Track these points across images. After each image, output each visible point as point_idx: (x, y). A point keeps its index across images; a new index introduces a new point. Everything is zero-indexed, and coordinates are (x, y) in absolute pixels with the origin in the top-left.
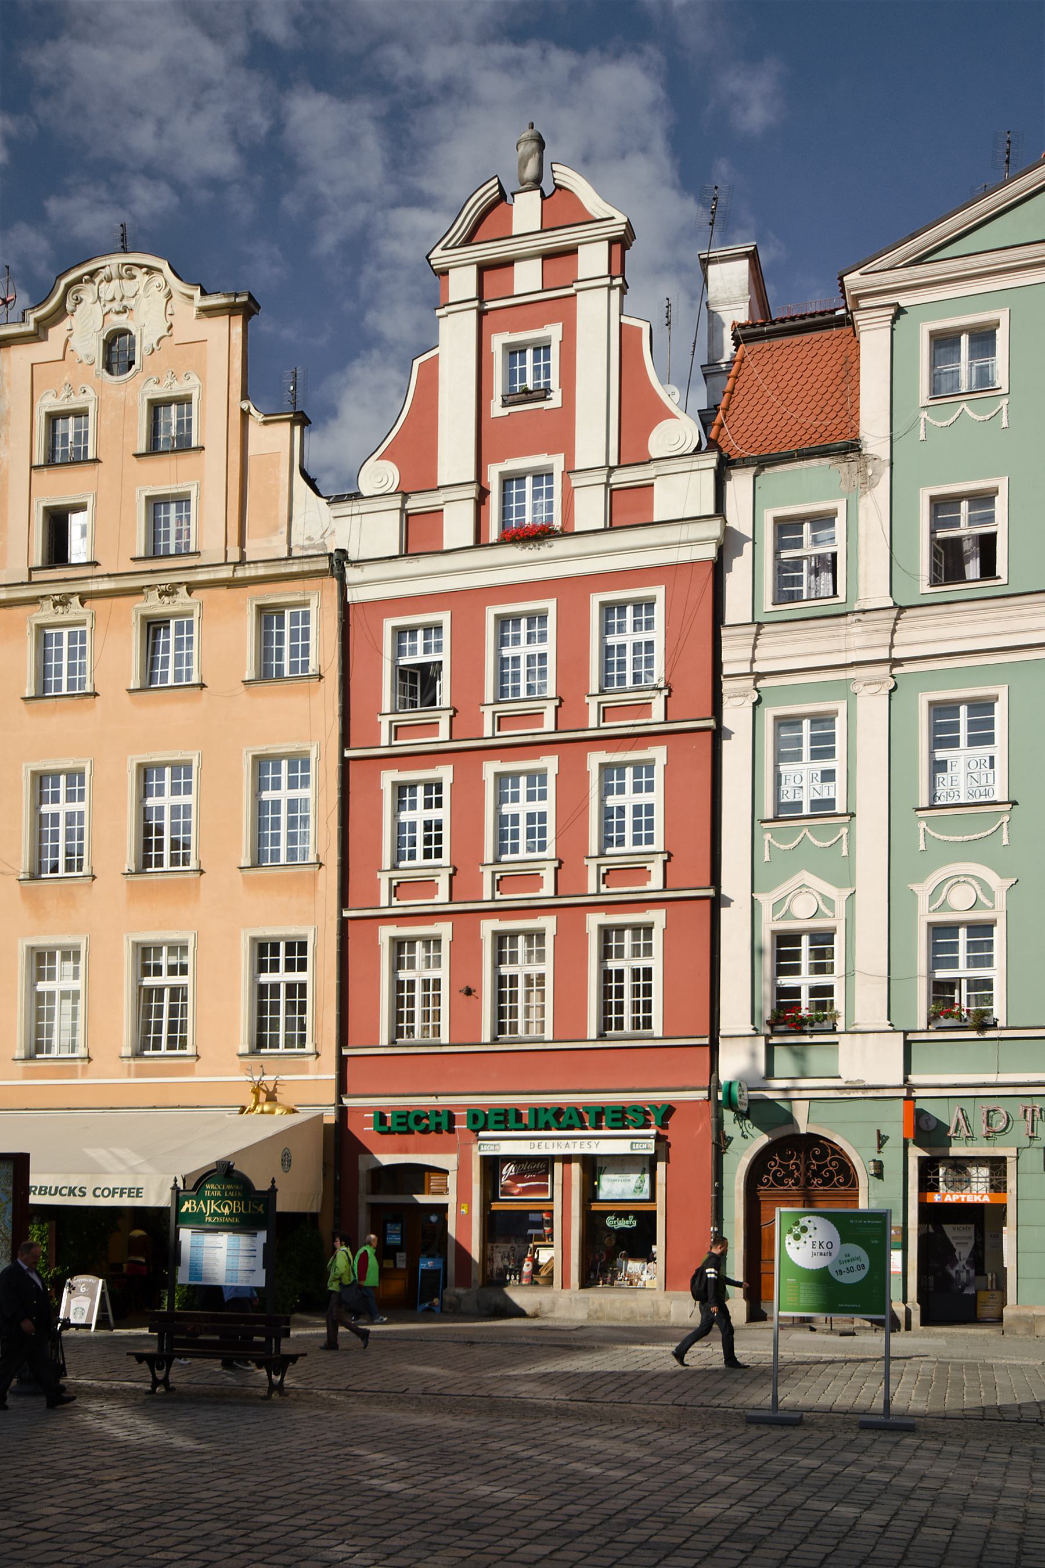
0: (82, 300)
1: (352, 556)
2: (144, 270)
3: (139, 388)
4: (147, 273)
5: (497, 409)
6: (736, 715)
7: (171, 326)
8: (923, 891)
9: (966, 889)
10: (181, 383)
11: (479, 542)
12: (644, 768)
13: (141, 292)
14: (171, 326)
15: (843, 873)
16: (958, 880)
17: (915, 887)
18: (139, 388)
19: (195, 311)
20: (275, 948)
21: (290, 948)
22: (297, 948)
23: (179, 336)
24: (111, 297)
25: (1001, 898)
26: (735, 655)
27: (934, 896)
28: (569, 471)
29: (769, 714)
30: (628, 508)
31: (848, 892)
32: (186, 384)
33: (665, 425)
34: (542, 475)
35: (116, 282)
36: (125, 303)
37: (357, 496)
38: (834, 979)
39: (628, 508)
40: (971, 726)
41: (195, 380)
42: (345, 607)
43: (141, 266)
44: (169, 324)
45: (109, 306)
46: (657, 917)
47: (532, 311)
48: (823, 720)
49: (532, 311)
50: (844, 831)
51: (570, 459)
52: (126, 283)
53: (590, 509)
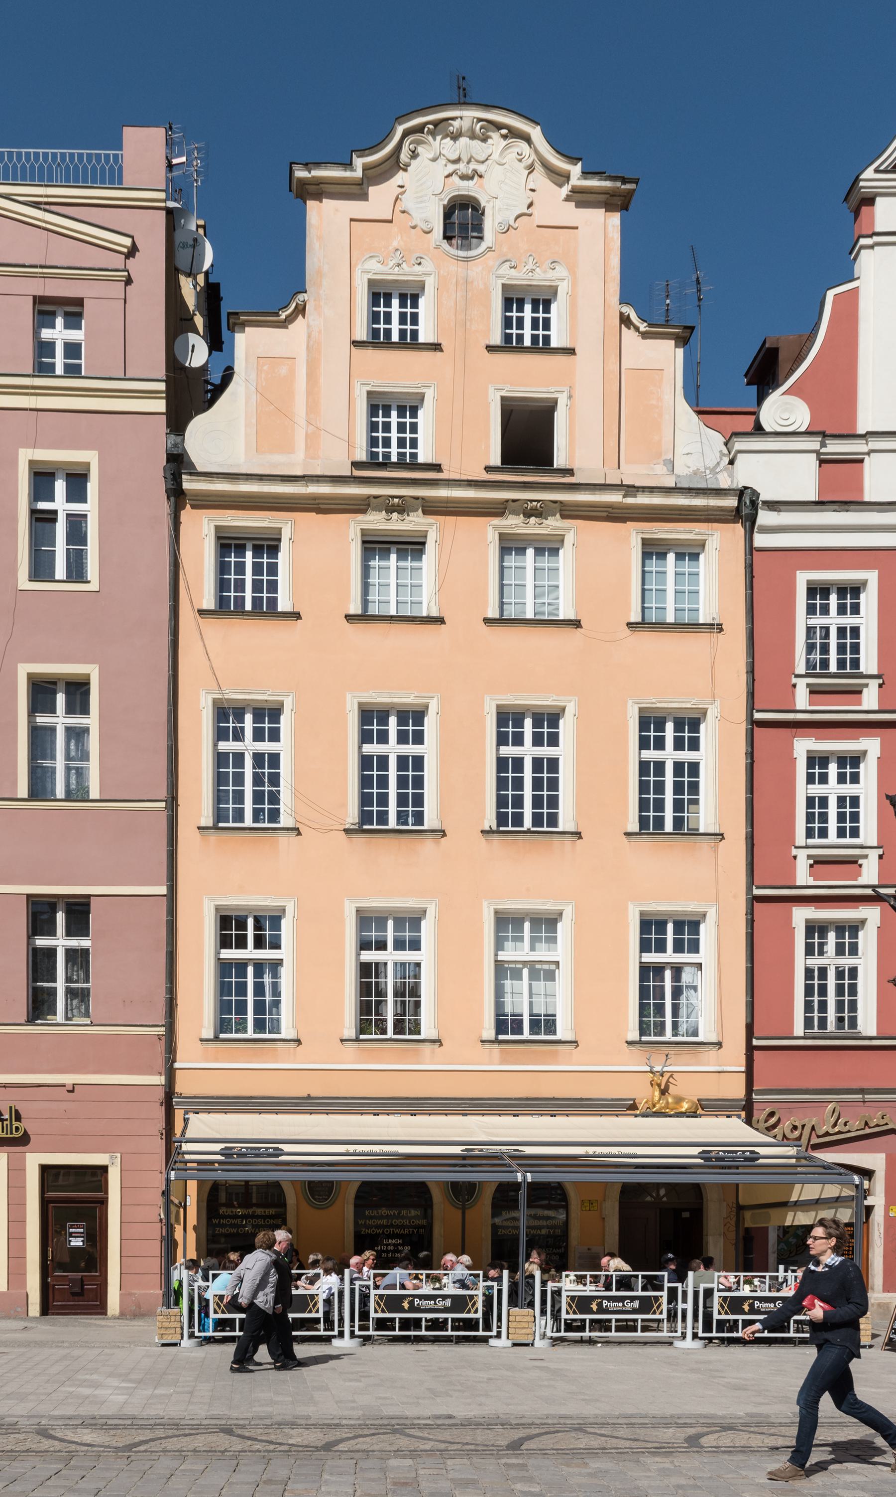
0: (418, 155)
2: (504, 131)
3: (488, 271)
4: (505, 137)
7: (530, 205)
10: (545, 272)
13: (495, 156)
14: (530, 205)
18: (488, 271)
19: (565, 190)
20: (661, 926)
23: (540, 215)
24: (454, 157)
32: (551, 275)
35: (463, 140)
36: (473, 166)
37: (759, 430)
43: (498, 126)
44: (529, 201)
45: (451, 168)
52: (476, 143)
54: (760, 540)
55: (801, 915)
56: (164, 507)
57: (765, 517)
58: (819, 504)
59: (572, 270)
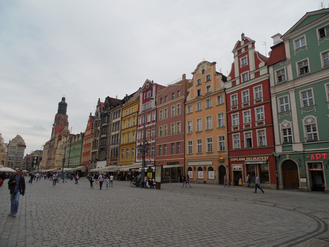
1: (227, 88)
5: (241, 67)
6: (273, 99)
8: (303, 120)
9: (310, 119)
11: (240, 83)
12: (261, 108)
15: (291, 119)
16: (310, 118)
17: (302, 120)
21: (223, 137)
22: (223, 137)
25: (316, 120)
26: (272, 91)
27: (305, 121)
28: (250, 72)
29: (278, 98)
30: (257, 75)
31: (292, 122)
33: (261, 63)
34: (247, 73)
38: (292, 135)
39: (257, 75)
40: (309, 94)
41: (210, 73)
42: (226, 94)
46: (265, 129)
47: (244, 54)
48: (286, 98)
49: (244, 54)
50: (290, 113)
51: (249, 71)
53: (253, 76)
54: (227, 93)
55: (233, 134)
56: (184, 105)
57: (226, 91)
58: (233, 87)
59: (211, 72)
